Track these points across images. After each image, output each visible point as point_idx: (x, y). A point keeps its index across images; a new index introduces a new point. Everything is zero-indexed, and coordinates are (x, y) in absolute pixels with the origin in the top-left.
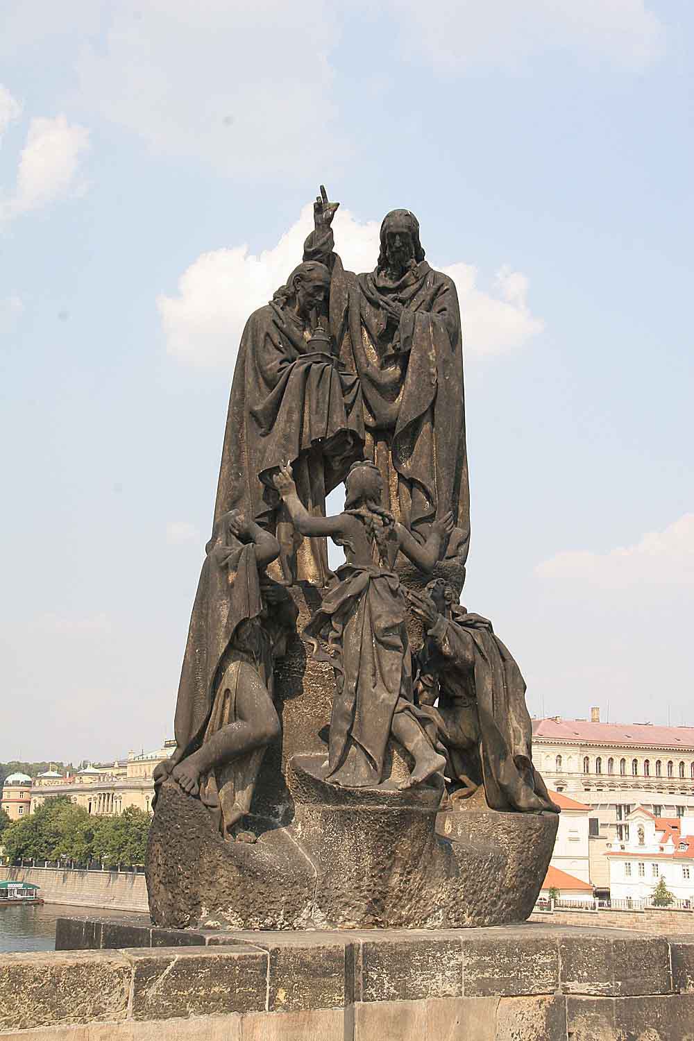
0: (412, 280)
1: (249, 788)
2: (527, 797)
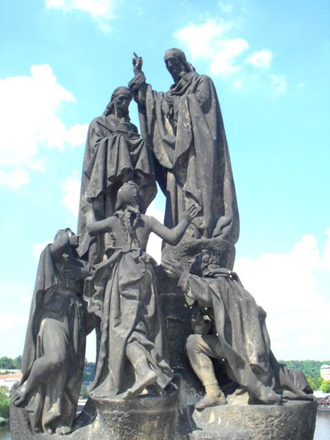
0: (184, 83)
1: (58, 400)
2: (267, 393)
